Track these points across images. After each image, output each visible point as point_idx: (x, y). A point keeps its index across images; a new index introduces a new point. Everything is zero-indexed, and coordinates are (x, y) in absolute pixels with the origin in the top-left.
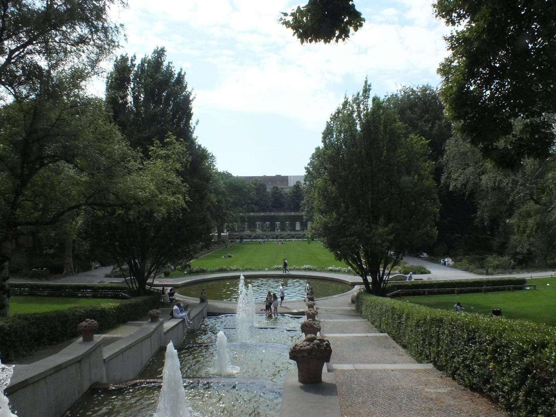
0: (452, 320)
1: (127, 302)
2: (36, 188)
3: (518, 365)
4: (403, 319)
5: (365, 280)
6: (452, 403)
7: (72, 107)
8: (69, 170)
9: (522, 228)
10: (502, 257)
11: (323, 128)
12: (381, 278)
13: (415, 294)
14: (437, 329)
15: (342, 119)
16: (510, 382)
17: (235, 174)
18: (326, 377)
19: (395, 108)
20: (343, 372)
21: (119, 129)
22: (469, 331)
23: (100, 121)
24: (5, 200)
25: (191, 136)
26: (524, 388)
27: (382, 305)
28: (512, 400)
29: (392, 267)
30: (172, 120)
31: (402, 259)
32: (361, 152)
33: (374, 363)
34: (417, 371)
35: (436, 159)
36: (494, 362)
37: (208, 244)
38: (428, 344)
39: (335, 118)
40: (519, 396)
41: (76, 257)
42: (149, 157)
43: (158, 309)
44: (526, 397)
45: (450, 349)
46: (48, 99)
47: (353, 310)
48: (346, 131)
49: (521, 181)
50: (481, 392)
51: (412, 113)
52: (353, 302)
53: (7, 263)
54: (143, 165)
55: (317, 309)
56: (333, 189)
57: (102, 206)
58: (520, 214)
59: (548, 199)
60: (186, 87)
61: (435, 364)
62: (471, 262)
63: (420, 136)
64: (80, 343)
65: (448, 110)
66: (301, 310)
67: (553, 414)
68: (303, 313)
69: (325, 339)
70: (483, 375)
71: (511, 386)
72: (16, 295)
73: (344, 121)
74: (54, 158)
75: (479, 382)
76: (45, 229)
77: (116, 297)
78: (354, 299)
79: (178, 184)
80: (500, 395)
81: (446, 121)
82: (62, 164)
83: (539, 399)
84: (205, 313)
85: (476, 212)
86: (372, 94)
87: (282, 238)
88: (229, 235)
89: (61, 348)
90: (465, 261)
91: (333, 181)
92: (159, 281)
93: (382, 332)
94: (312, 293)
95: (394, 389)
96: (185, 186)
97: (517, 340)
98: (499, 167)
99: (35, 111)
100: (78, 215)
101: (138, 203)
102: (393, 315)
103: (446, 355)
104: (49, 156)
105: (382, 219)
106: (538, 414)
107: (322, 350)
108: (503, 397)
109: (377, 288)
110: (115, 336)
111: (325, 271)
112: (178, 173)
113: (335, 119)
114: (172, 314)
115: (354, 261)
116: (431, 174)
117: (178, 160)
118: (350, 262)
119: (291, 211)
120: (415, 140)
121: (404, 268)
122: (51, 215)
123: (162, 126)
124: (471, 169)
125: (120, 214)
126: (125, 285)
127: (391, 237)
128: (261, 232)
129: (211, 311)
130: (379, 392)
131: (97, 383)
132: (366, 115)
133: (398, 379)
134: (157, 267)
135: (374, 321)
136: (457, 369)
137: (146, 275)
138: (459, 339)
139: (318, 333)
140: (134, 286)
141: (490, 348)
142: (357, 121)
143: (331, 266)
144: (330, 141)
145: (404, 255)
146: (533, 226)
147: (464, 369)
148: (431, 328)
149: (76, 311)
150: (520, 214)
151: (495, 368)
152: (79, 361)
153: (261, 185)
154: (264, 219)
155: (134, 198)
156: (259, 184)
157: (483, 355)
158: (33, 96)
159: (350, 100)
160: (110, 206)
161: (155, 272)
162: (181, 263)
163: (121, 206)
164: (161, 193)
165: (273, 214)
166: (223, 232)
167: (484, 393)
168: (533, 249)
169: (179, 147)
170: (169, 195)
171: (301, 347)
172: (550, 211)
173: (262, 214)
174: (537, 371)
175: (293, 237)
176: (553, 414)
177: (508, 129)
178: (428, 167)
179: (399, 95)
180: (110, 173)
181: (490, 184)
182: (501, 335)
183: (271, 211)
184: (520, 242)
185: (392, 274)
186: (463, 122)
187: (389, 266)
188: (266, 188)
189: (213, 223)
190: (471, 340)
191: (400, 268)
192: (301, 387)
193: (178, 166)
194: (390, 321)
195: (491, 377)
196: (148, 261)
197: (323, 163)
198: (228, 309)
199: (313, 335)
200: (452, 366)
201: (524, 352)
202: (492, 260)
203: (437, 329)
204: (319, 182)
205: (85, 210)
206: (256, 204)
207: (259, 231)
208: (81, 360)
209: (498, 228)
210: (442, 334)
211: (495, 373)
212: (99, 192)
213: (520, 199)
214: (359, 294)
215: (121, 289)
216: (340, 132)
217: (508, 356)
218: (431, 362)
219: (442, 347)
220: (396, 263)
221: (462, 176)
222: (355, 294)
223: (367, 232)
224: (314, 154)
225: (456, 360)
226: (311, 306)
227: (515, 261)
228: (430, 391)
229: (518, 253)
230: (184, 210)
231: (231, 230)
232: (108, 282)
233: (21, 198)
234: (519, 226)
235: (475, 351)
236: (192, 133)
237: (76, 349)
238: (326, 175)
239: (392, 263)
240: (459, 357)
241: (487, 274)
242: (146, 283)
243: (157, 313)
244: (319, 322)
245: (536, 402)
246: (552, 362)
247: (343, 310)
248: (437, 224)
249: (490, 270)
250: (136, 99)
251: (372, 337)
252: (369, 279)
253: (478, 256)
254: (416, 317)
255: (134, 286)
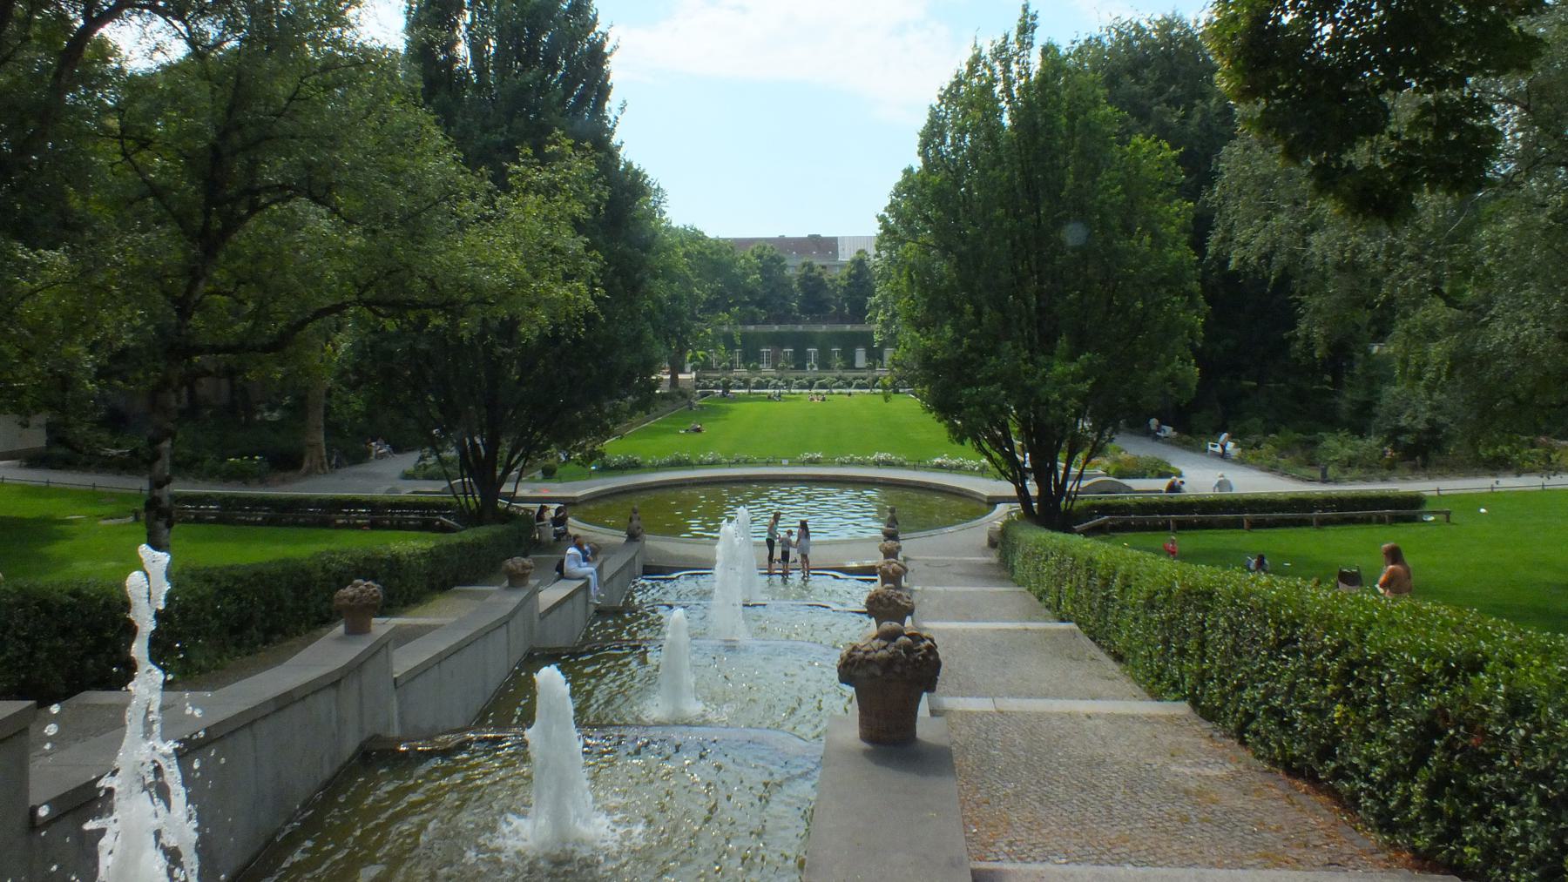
0: (1237, 593)
1: (454, 538)
2: (240, 263)
3: (1406, 714)
4: (1115, 589)
5: (1022, 491)
6: (1239, 803)
7: (325, 69)
8: (319, 221)
9: (1411, 366)
10: (1361, 437)
11: (922, 121)
12: (1061, 488)
13: (1142, 528)
14: (1200, 615)
15: (969, 98)
16: (1388, 756)
17: (711, 234)
18: (927, 727)
19: (1095, 71)
20: (968, 716)
21: (437, 122)
22: (1279, 623)
23: (393, 103)
24: (164, 293)
25: (609, 139)
26: (1424, 773)
27: (1063, 553)
28: (1393, 804)
29: (1088, 461)
30: (563, 102)
31: (1111, 440)
32: (1011, 179)
33: (1046, 696)
34: (1150, 720)
35: (1191, 192)
36: (1344, 704)
37: (647, 401)
38: (1183, 654)
39: (951, 95)
40: (1411, 794)
41: (333, 429)
42: (507, 189)
43: (525, 556)
44: (1431, 799)
45: (1232, 668)
46: (269, 49)
47: (990, 564)
48: (975, 130)
49: (1410, 249)
50: (1313, 779)
51: (1137, 83)
52: (993, 544)
53: (166, 444)
54: (494, 208)
55: (906, 559)
56: (943, 267)
57: (398, 307)
58: (1408, 332)
59: (1481, 293)
60: (594, 22)
61: (1195, 702)
62: (1284, 450)
63: (1157, 140)
64: (339, 639)
65: (1227, 74)
66: (868, 563)
67: (1503, 847)
68: (871, 571)
69: (925, 634)
70: (1317, 735)
71: (1391, 767)
72: (187, 521)
73: (972, 105)
74: (283, 192)
75: (1308, 754)
76: (260, 363)
77: (426, 526)
78: (996, 538)
79: (575, 254)
80: (1361, 789)
81: (1219, 101)
82: (302, 205)
83: (1465, 804)
84: (638, 569)
85: (1295, 327)
86: (1040, 39)
87: (822, 386)
88: (697, 379)
89: (293, 652)
90: (1267, 448)
91: (946, 249)
92: (528, 490)
93: (1063, 620)
94: (893, 521)
95: (1094, 764)
96: (594, 259)
97: (1403, 648)
98: (1355, 215)
99: (238, 77)
100: (339, 329)
101: (483, 301)
102: (1090, 577)
103: (1223, 683)
104: (269, 188)
105: (1063, 343)
106: (1465, 844)
107: (916, 660)
108: (1371, 795)
109: (1052, 512)
110: (421, 621)
111: (925, 468)
112: (578, 226)
113: (950, 100)
114: (560, 567)
115: (995, 442)
116: (1185, 231)
117: (578, 195)
118: (986, 446)
119: (843, 320)
120: (1145, 150)
121: (1118, 461)
122: (273, 329)
123: (538, 116)
124: (1283, 219)
125: (437, 327)
126: (449, 498)
127: (1085, 387)
128: (773, 372)
129: (654, 562)
130: (1056, 770)
131: (376, 738)
132: (1025, 89)
133: (1103, 738)
134: (526, 456)
135: (1044, 592)
136: (1251, 717)
137: (499, 473)
138: (1254, 642)
139: (908, 620)
140: (471, 500)
141: (1334, 666)
142: (1003, 104)
143: (941, 456)
144: (940, 152)
145: (1116, 430)
146: (1443, 363)
147: (1268, 718)
148: (1183, 612)
149: (332, 561)
150: (1408, 332)
151: (1347, 718)
152: (334, 682)
153: (773, 259)
155: (472, 288)
156: (771, 255)
157: (1315, 684)
158: (234, 43)
159: (986, 51)
160: (415, 306)
161: (519, 467)
162: (583, 446)
163: (442, 307)
164: (536, 276)
165: (800, 328)
166: (683, 372)
167: (1320, 781)
168: (1441, 419)
169: (579, 166)
170: (555, 281)
171: (867, 652)
172: (1485, 325)
173: (776, 328)
174: (1457, 732)
175: (849, 385)
176: (1503, 847)
177: (1374, 121)
178: (1177, 215)
179: (1105, 40)
180: (413, 226)
181: (1333, 257)
182: (1361, 637)
183: (797, 321)
184: (1410, 403)
185: (1087, 477)
186: (1263, 102)
187: (1081, 456)
188: (784, 267)
189: (659, 350)
190: (1285, 644)
191: (1107, 463)
192: (866, 753)
193: (578, 209)
194: (1083, 593)
195: (1337, 742)
196: (503, 440)
197: (920, 207)
198: (694, 558)
199: (895, 624)
200: (1236, 711)
201: (1424, 680)
202: (1336, 445)
203: (1200, 615)
204: (910, 251)
205: (355, 315)
206: (761, 304)
207: (767, 371)
208: (338, 681)
209: (1351, 366)
210: (1211, 627)
211: (1349, 731)
212: (390, 272)
213: (1407, 295)
214: (1007, 525)
215: (441, 507)
216: (962, 130)
217: (1380, 688)
218: (1184, 698)
219: (1213, 661)
220: (1097, 450)
221: (1261, 234)
222: (998, 524)
223: (1026, 373)
224: (899, 184)
225: (1247, 694)
226: (890, 554)
227: (1395, 449)
228: (1182, 770)
229: (1402, 431)
230: (590, 319)
231: (705, 366)
232: (407, 490)
233: (202, 287)
234: (1405, 362)
235: (1296, 674)
236: (611, 132)
237: (325, 654)
238: (927, 235)
239: (1087, 450)
240: (1255, 688)
241: (1325, 480)
242: (497, 495)
243: (524, 567)
244: (912, 591)
245: (1457, 811)
246: (1498, 710)
247: (969, 564)
248: (1198, 354)
249: (1331, 471)
250: (477, 49)
251: (1040, 631)
252: (1033, 488)
253: (1299, 436)
254: (1147, 584)
255: (471, 500)
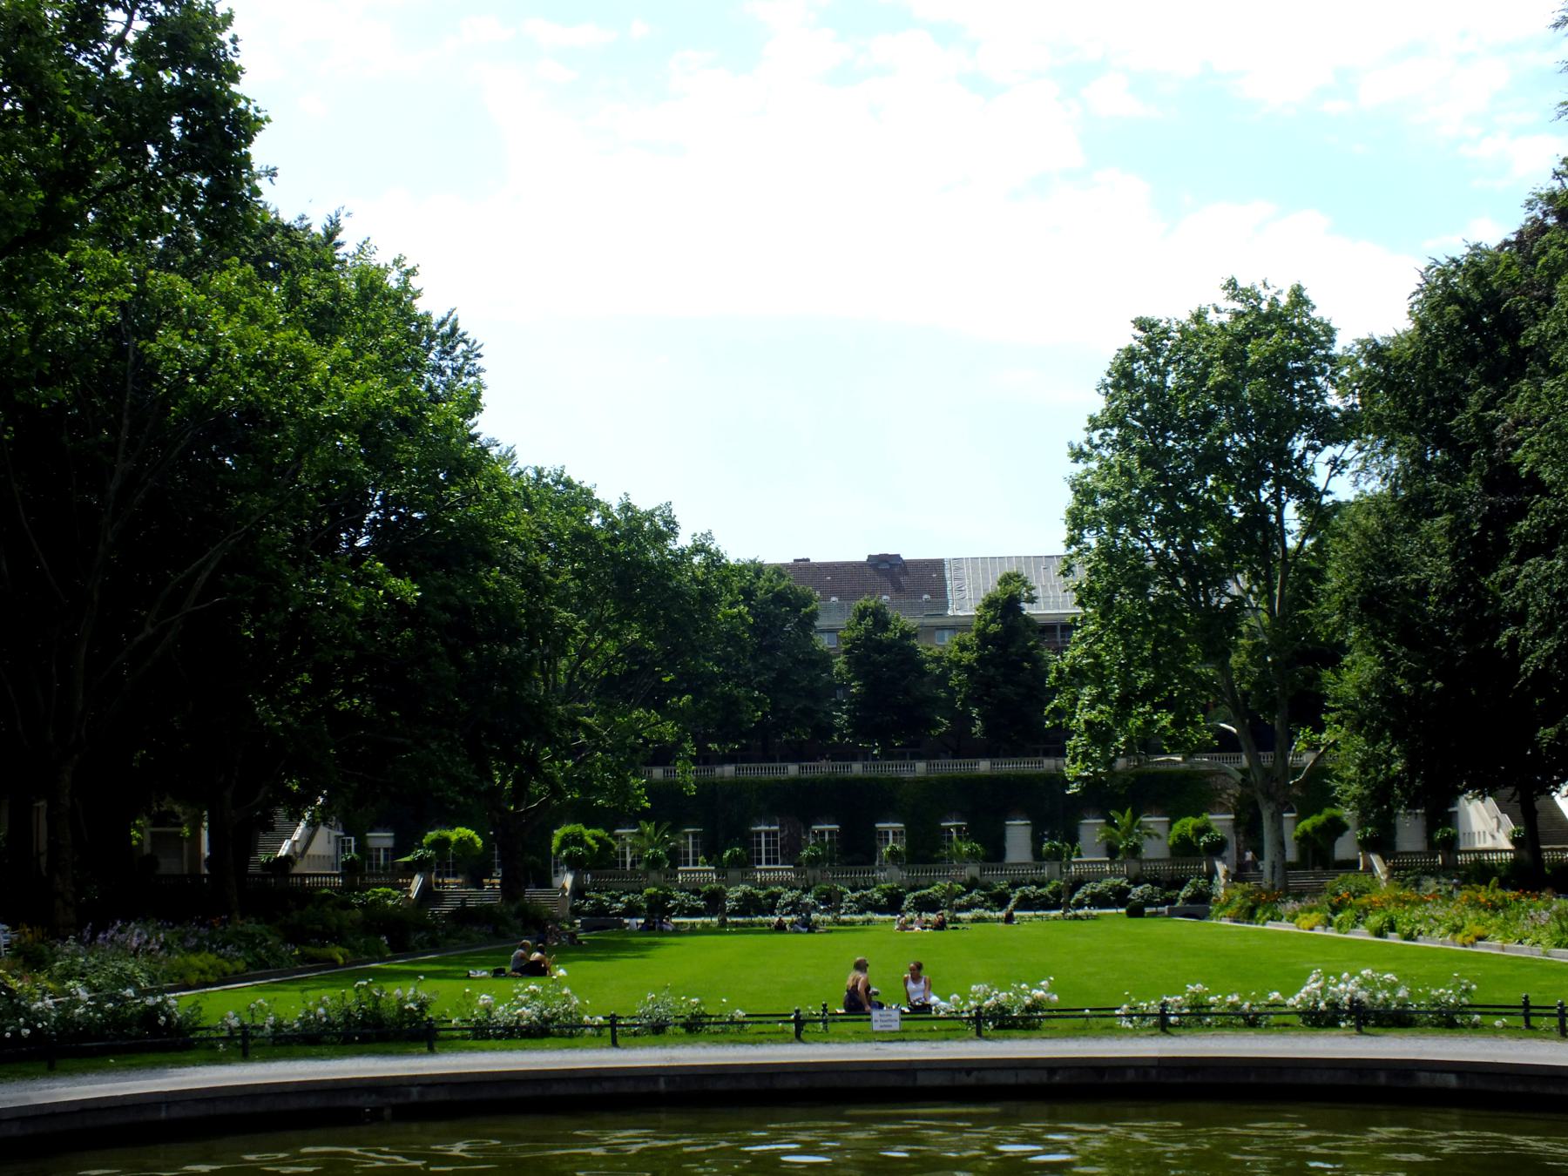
153: (780, 598)
154: (799, 804)
165: (857, 768)
173: (793, 769)
